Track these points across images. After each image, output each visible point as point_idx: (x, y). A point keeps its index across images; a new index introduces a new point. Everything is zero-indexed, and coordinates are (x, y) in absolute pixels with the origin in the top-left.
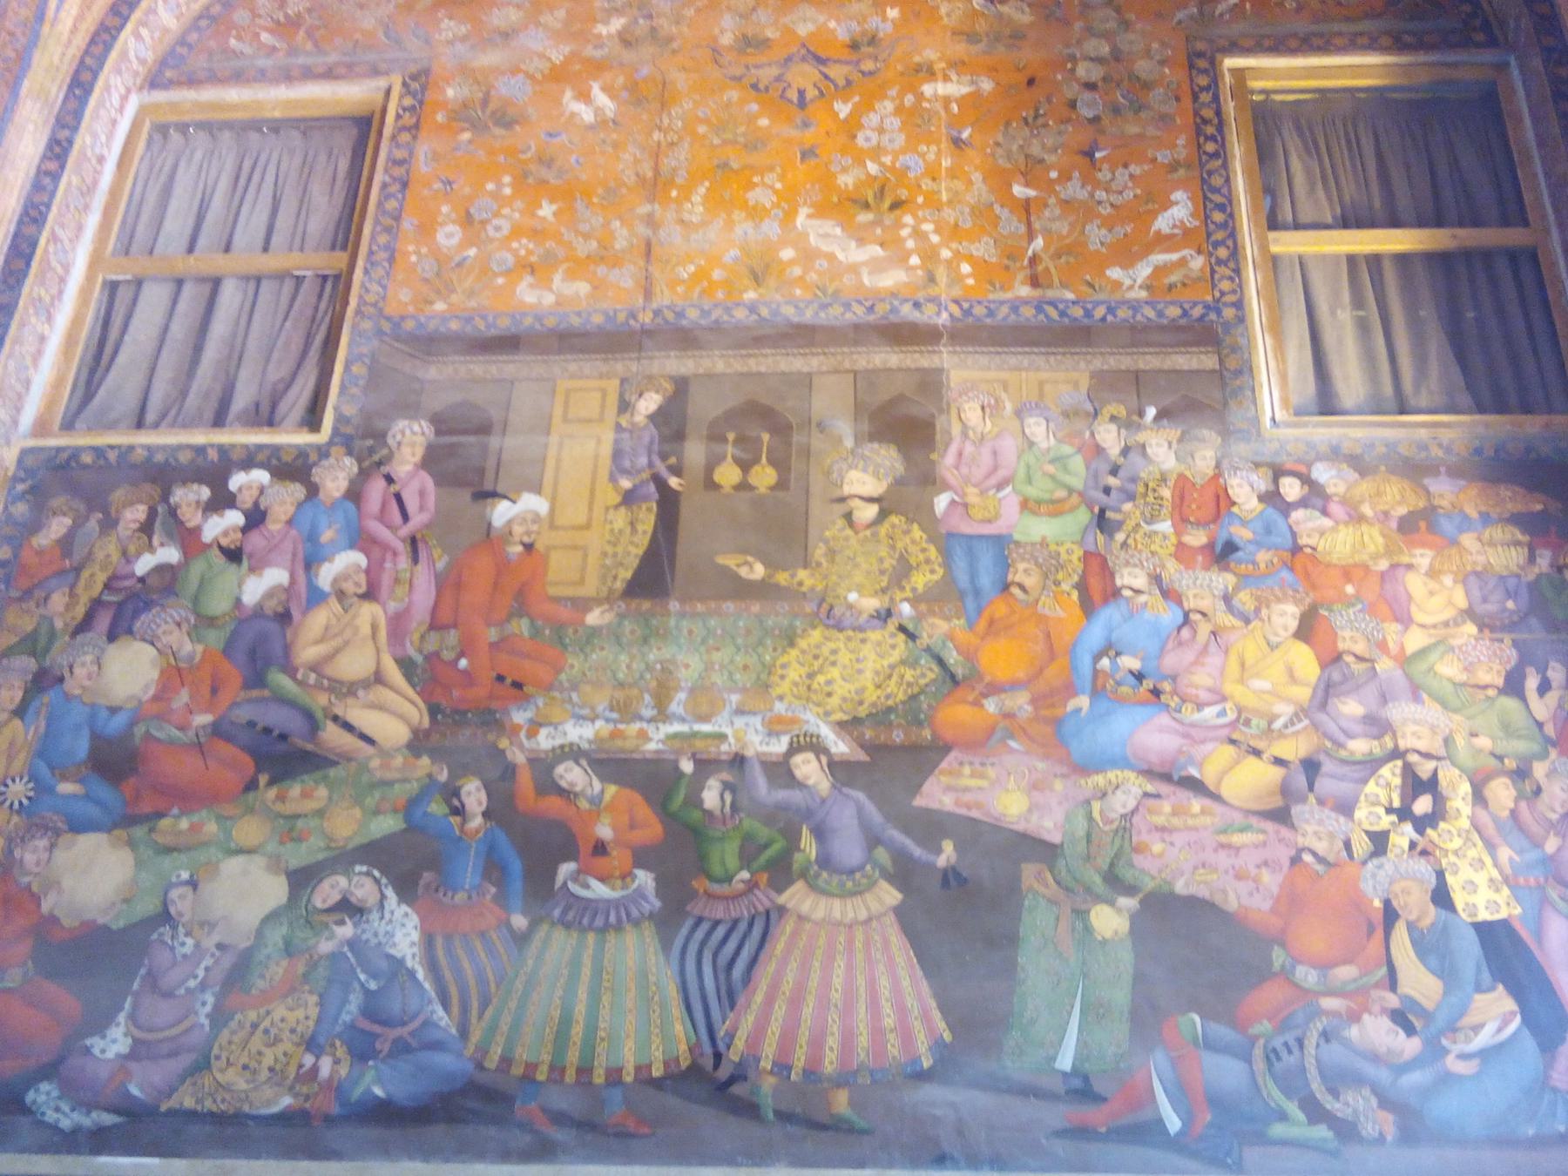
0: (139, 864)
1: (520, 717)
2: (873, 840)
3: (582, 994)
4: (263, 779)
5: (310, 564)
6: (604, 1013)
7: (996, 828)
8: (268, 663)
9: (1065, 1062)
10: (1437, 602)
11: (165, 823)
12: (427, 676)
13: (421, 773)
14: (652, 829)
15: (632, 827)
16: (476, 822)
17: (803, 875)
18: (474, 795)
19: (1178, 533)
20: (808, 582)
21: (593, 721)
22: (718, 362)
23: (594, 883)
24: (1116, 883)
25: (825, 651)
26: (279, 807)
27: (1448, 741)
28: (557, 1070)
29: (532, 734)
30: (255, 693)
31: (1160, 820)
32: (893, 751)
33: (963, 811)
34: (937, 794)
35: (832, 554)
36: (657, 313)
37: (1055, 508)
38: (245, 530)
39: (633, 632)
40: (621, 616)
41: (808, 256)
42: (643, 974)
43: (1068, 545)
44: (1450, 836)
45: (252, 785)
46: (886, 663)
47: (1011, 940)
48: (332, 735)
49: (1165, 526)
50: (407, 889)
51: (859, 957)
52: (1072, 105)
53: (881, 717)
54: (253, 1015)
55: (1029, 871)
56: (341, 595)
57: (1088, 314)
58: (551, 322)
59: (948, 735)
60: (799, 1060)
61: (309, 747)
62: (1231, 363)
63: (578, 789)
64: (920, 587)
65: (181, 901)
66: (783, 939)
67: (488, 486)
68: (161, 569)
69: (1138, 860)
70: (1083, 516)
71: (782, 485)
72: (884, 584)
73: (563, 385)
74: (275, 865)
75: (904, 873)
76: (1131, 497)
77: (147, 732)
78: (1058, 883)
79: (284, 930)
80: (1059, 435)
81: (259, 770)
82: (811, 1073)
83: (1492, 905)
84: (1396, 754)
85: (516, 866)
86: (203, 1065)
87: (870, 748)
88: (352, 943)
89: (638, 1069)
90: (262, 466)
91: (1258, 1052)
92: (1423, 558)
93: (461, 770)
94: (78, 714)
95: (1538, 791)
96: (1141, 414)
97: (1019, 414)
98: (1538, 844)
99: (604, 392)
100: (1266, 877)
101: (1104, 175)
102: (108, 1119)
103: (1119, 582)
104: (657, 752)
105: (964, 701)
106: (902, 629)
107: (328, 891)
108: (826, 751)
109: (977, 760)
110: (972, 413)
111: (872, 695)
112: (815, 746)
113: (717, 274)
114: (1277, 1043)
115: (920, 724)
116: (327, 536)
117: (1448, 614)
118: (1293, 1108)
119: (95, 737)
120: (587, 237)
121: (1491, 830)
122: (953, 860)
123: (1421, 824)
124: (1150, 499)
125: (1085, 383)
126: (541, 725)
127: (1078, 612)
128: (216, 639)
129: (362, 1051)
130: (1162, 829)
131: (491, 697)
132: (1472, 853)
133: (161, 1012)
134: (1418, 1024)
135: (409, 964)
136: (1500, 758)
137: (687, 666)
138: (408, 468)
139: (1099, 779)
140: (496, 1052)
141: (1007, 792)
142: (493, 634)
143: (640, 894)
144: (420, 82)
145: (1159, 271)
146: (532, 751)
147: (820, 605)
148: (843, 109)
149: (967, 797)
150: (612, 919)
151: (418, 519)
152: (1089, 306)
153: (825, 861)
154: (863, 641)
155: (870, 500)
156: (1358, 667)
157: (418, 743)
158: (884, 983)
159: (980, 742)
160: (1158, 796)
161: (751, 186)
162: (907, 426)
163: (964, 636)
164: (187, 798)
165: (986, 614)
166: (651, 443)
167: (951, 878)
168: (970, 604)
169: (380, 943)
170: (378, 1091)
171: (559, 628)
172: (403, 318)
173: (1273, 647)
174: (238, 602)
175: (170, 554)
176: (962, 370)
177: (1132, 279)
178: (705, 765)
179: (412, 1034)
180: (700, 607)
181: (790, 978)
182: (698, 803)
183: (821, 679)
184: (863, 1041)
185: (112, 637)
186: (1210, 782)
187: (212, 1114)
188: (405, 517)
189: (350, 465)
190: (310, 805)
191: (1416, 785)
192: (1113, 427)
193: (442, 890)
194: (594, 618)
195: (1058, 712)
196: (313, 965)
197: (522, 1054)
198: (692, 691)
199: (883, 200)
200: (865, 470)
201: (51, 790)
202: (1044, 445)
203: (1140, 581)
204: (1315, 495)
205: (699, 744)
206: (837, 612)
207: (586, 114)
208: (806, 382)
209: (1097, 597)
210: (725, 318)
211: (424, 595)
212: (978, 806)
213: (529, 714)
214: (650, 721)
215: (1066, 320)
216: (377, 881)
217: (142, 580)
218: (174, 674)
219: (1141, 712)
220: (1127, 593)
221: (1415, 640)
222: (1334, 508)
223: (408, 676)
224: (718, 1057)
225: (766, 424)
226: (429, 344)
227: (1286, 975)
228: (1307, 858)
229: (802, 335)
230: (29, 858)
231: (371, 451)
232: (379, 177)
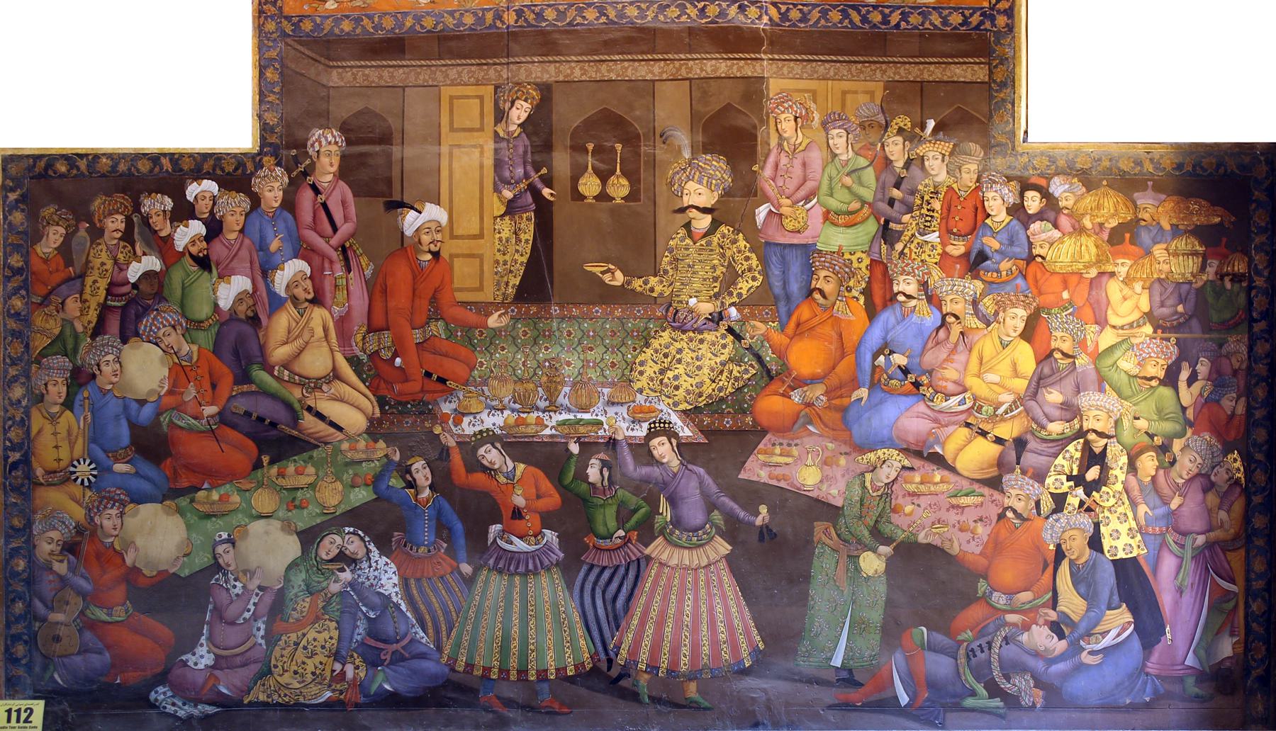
0: (189, 527)
1: (447, 408)
2: (711, 506)
3: (515, 620)
4: (266, 459)
5: (266, 270)
7: (798, 495)
8: (250, 362)
9: (837, 661)
10: (1129, 304)
11: (201, 494)
12: (373, 371)
13: (380, 454)
14: (553, 499)
15: (539, 497)
17: (662, 533)
18: (421, 471)
19: (943, 244)
20: (658, 289)
21: (502, 410)
22: (574, 69)
23: (514, 539)
24: (879, 536)
25: (673, 350)
26: (281, 481)
27: (1117, 423)
28: (504, 672)
29: (458, 423)
30: (245, 388)
31: (912, 488)
32: (726, 433)
33: (774, 482)
34: (756, 470)
36: (519, 13)
37: (849, 219)
38: (209, 238)
39: (525, 334)
40: (515, 319)
42: (555, 605)
43: (859, 255)
45: (258, 465)
46: (718, 360)
47: (807, 578)
49: (933, 237)
50: (385, 549)
51: (703, 592)
53: (715, 406)
54: (293, 637)
55: (819, 527)
56: (295, 300)
57: (885, 21)
58: (429, 23)
59: (765, 421)
61: (295, 433)
62: (999, 77)
63: (496, 467)
64: (744, 292)
65: (227, 556)
66: (650, 580)
67: (397, 197)
68: (148, 275)
69: (895, 518)
70: (872, 227)
71: (632, 197)
72: (716, 290)
73: (447, 92)
74: (287, 527)
75: (732, 530)
76: (910, 210)
77: (171, 421)
78: (838, 536)
79: (303, 575)
80: (857, 147)
81: (261, 452)
82: (671, 671)
85: (459, 527)
86: (267, 672)
88: (352, 584)
89: (557, 670)
91: (962, 651)
92: (1123, 267)
93: (408, 453)
94: (113, 407)
95: (1173, 463)
96: (923, 127)
97: (824, 125)
98: (1166, 503)
99: (481, 98)
100: (980, 529)
102: (210, 710)
103: (896, 289)
104: (552, 436)
105: (776, 393)
106: (730, 330)
107: (329, 546)
108: (676, 435)
109: (785, 442)
110: (787, 126)
111: (708, 389)
112: (670, 433)
114: (975, 645)
115: (744, 412)
116: (274, 245)
117: (1135, 316)
118: (980, 689)
119: (133, 426)
121: (1136, 492)
122: (767, 521)
123: (1091, 488)
124: (924, 211)
125: (879, 95)
126: (464, 415)
127: (863, 315)
128: (206, 338)
129: (373, 662)
130: (913, 494)
131: (422, 391)
132: (1121, 510)
133: (230, 636)
134: (1067, 632)
135: (395, 599)
136: (1151, 436)
137: (569, 364)
138: (330, 178)
139: (872, 456)
140: (462, 660)
141: (804, 467)
142: (417, 336)
143: (548, 548)
146: (459, 436)
147: (667, 310)
149: (778, 471)
150: (531, 567)
151: (345, 229)
152: (887, 11)
153: (677, 522)
154: (701, 341)
155: (705, 210)
156: (1063, 363)
157: (374, 430)
158: (719, 609)
159: (789, 428)
160: (912, 469)
162: (733, 136)
163: (778, 338)
164: (216, 476)
165: (794, 318)
166: (525, 152)
167: (765, 533)
168: (782, 304)
169: (372, 585)
170: (387, 687)
171: (468, 328)
172: (302, 18)
173: (1004, 346)
174: (216, 306)
175: (152, 263)
178: (588, 447)
179: (403, 648)
180: (575, 312)
181: (656, 606)
183: (670, 374)
185: (124, 340)
186: (949, 458)
187: (278, 704)
188: (335, 229)
190: (304, 480)
191: (1093, 458)
192: (900, 139)
193: (409, 545)
195: (845, 401)
196: (328, 601)
197: (480, 662)
198: (574, 384)
200: (700, 182)
202: (844, 157)
203: (911, 288)
205: (582, 430)
206: (681, 315)
208: (648, 89)
209: (878, 300)
210: (579, 20)
211: (360, 302)
212: (785, 478)
213: (453, 406)
214: (544, 412)
215: (867, 26)
216: (362, 539)
217: (135, 286)
218: (180, 372)
219: (905, 401)
220: (901, 298)
221: (1108, 338)
222: (1064, 221)
223: (359, 374)
224: (610, 661)
225: (618, 134)
227: (986, 599)
228: (1010, 514)
229: (643, 40)
230: (107, 523)
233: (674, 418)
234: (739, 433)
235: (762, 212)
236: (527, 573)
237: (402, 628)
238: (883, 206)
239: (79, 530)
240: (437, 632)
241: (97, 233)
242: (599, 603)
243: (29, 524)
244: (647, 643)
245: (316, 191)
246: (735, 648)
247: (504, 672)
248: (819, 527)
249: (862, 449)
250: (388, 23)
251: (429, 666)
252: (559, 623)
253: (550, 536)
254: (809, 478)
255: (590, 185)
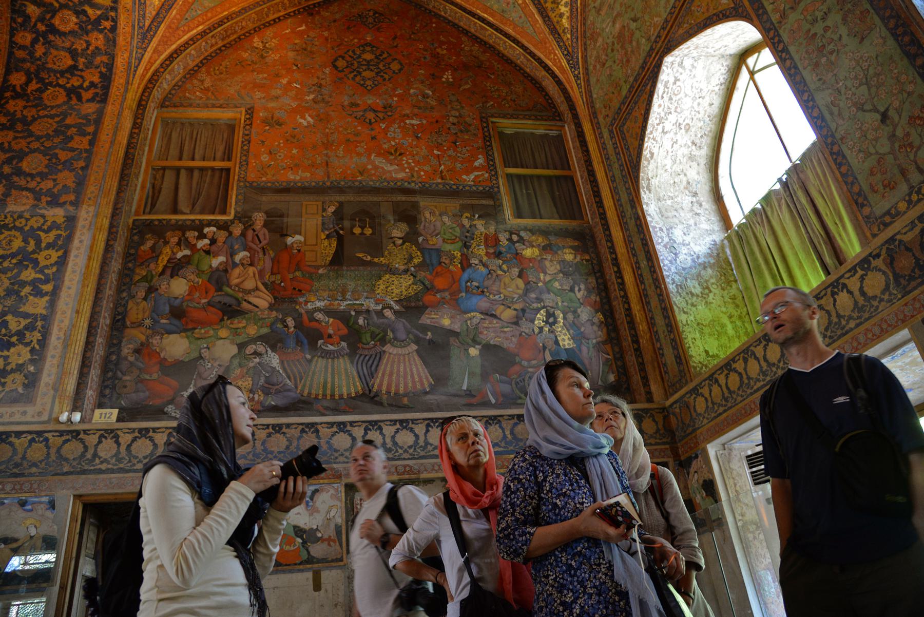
0: (190, 343)
1: (301, 300)
2: (408, 333)
3: (329, 376)
4: (226, 318)
5: (232, 254)
6: (336, 380)
9: (465, 387)
12: (271, 288)
14: (345, 331)
16: (292, 329)
17: (389, 342)
18: (290, 322)
22: (350, 197)
24: (475, 342)
28: (324, 396)
32: (412, 307)
35: (390, 253)
38: (210, 245)
40: (329, 271)
41: (376, 168)
42: (346, 370)
44: (559, 327)
45: (222, 320)
47: (449, 357)
48: (245, 305)
49: (483, 247)
50: (274, 348)
51: (407, 363)
52: (449, 129)
53: (408, 299)
55: (452, 339)
56: (243, 264)
58: (299, 184)
60: (393, 390)
65: (205, 353)
68: (184, 256)
69: (481, 336)
70: (460, 244)
74: (232, 343)
75: (417, 341)
76: (473, 239)
82: (396, 394)
83: (569, 344)
84: (544, 307)
85: (305, 341)
87: (406, 308)
90: (213, 226)
93: (286, 315)
97: (440, 215)
100: (513, 339)
101: (459, 149)
107: (250, 349)
110: (427, 215)
111: (405, 293)
112: (391, 308)
113: (349, 172)
116: (236, 247)
119: (171, 306)
120: (308, 159)
123: (551, 324)
128: (206, 277)
129: (267, 393)
142: (291, 276)
144: (250, 111)
145: (476, 177)
148: (383, 126)
151: (264, 242)
153: (395, 338)
157: (271, 307)
158: (414, 369)
159: (436, 305)
161: (357, 147)
162: (409, 216)
163: (429, 277)
164: (203, 324)
167: (431, 342)
175: (187, 252)
176: (423, 202)
177: (469, 178)
178: (358, 313)
181: (388, 369)
182: (358, 323)
184: (410, 385)
185: (172, 277)
189: (241, 226)
190: (241, 325)
191: (549, 315)
194: (321, 271)
196: (248, 370)
197: (314, 392)
199: (396, 153)
201: (159, 322)
203: (477, 262)
204: (521, 240)
207: (305, 124)
208: (378, 204)
209: (465, 265)
211: (268, 265)
218: (193, 289)
219: (479, 297)
221: (548, 278)
222: (526, 243)
223: (266, 288)
224: (370, 391)
225: (367, 215)
226: (262, 190)
227: (520, 363)
230: (155, 342)
231: (247, 222)
232: (240, 140)
233: (392, 303)
234: (417, 307)
235: (420, 239)
236: (333, 359)
237: (280, 380)
238: (464, 238)
239: (142, 344)
240: (295, 380)
241: (166, 243)
242: (365, 368)
243: (120, 342)
244: (385, 383)
245: (254, 230)
246: (422, 384)
247: (324, 396)
248: (452, 339)
249: (466, 313)
250: (284, 184)
251: (292, 394)
252: (347, 376)
253: (344, 344)
254: (446, 322)
255: (357, 231)
